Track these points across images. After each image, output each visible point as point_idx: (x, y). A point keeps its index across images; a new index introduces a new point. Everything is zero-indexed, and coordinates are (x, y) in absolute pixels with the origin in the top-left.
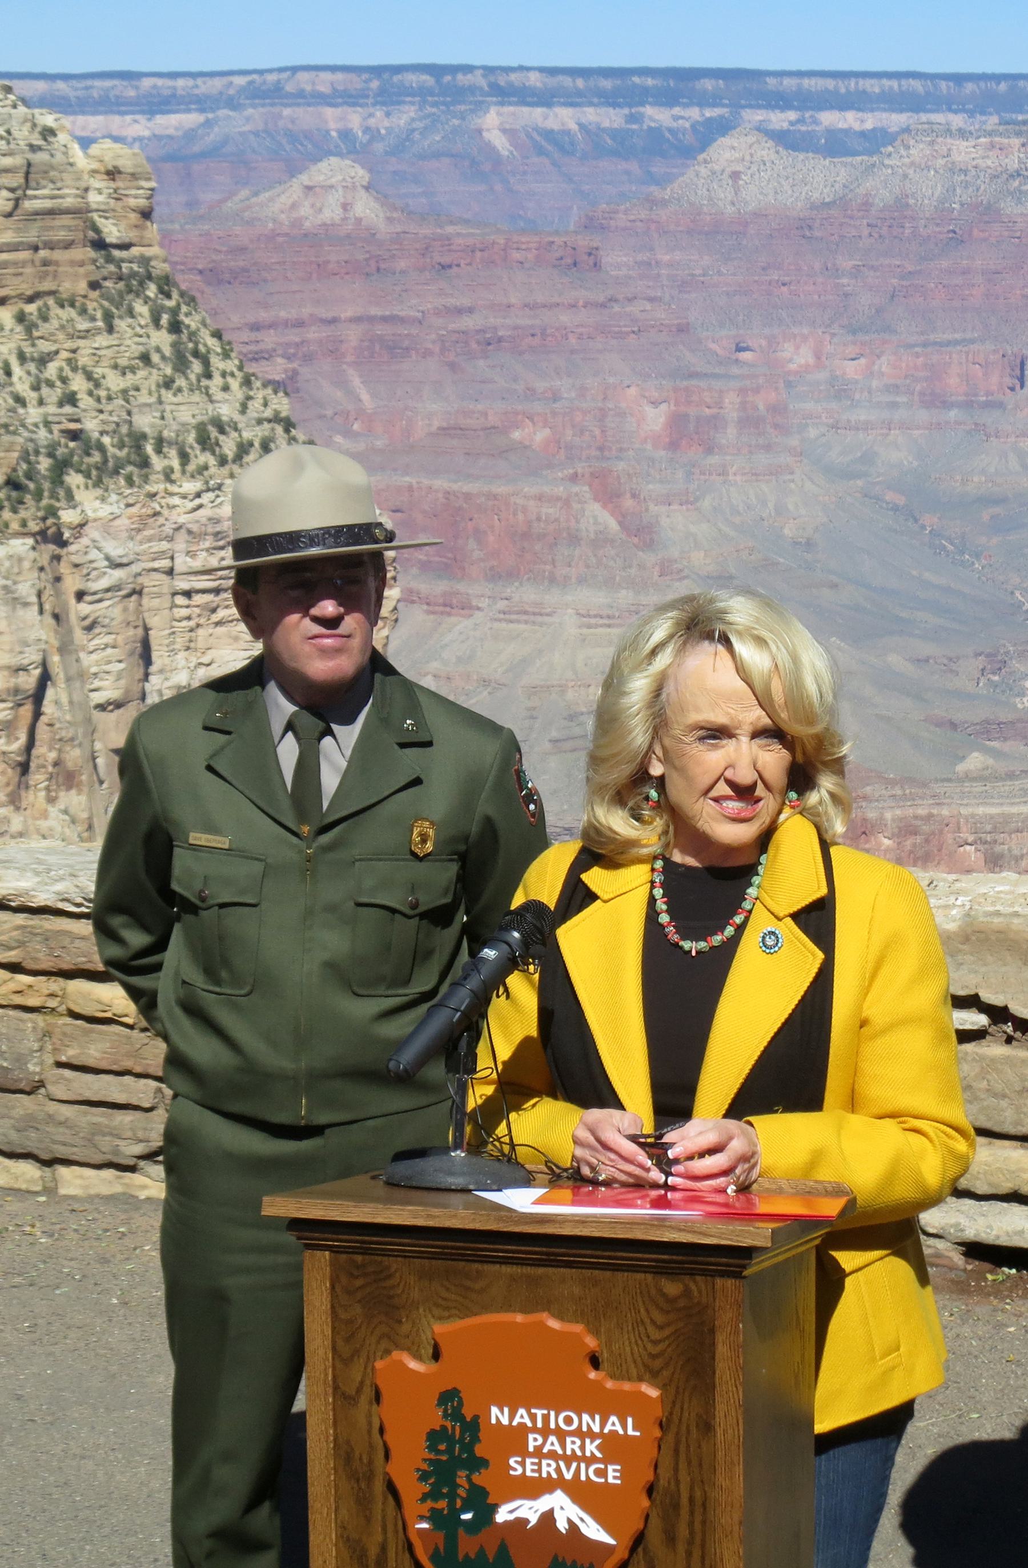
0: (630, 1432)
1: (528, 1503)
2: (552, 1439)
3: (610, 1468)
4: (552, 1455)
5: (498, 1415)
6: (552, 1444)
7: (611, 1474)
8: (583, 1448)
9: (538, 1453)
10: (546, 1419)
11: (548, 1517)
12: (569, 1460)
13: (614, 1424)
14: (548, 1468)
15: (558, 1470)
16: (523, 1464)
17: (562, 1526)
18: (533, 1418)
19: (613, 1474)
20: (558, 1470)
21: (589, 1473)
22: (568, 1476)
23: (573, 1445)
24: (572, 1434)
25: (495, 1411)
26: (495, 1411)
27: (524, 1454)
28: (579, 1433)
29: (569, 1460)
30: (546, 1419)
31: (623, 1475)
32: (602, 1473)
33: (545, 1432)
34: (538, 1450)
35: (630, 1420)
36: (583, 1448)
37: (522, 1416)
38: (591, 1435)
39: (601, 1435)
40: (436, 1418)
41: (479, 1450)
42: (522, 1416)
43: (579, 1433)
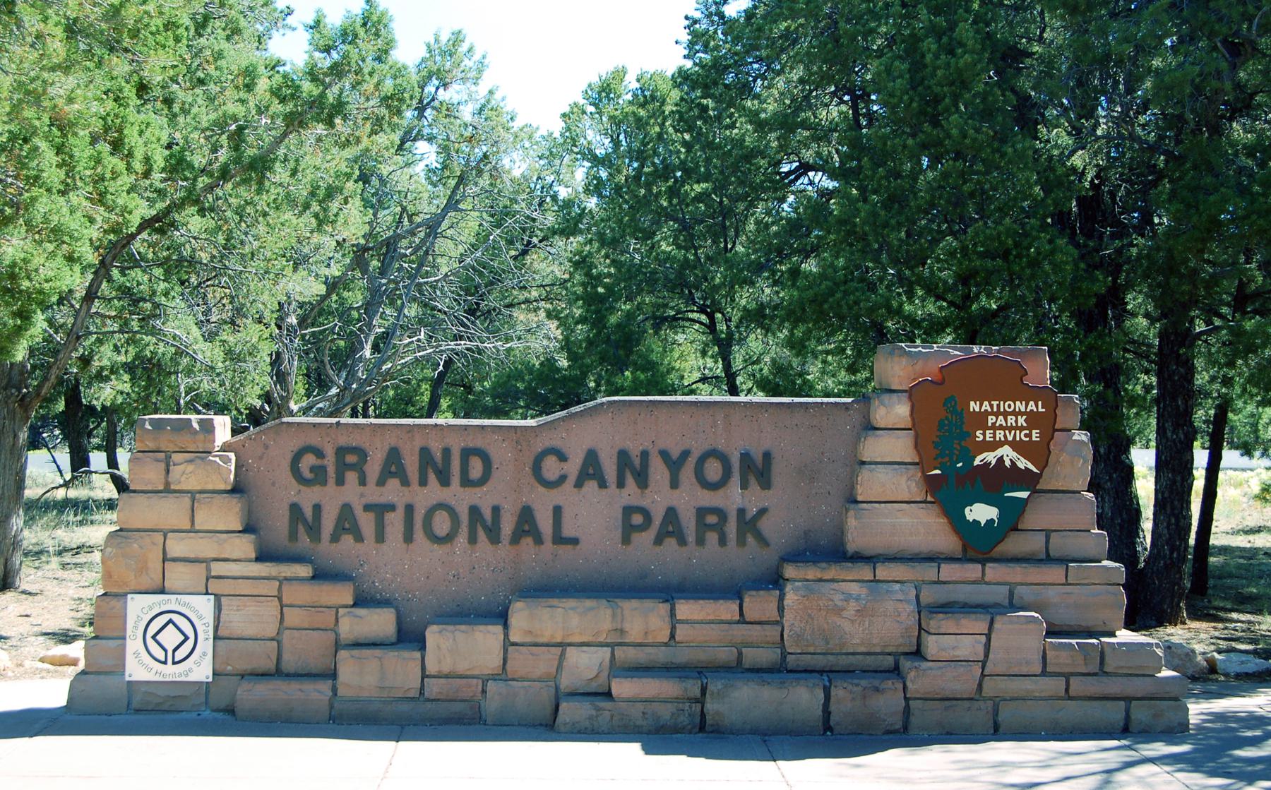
2: (1001, 417)
4: (1001, 427)
6: (1001, 421)
7: (1034, 435)
8: (1016, 421)
10: (998, 406)
11: (1001, 460)
12: (1010, 428)
14: (1000, 435)
15: (1005, 436)
16: (984, 434)
17: (1008, 463)
18: (992, 406)
20: (1005, 436)
21: (1021, 436)
22: (1010, 438)
23: (1011, 420)
25: (972, 403)
26: (972, 403)
27: (985, 428)
29: (1010, 428)
30: (998, 406)
32: (1029, 435)
33: (997, 414)
34: (994, 424)
36: (1016, 421)
37: (986, 404)
43: (1016, 414)
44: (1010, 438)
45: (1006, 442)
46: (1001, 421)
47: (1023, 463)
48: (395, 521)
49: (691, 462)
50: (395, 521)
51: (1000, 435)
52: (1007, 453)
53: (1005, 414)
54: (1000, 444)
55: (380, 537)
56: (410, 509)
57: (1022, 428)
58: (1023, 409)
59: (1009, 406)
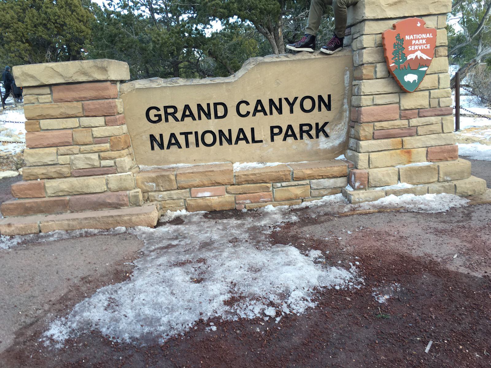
0: (431, 37)
1: (413, 54)
2: (417, 41)
3: (428, 45)
4: (417, 45)
5: (407, 38)
6: (417, 42)
9: (414, 45)
10: (416, 36)
11: (417, 56)
13: (428, 36)
14: (416, 47)
15: (418, 48)
17: (419, 57)
18: (414, 37)
19: (428, 46)
20: (418, 48)
21: (424, 47)
22: (420, 48)
23: (421, 41)
24: (421, 39)
25: (407, 37)
26: (407, 37)
27: (412, 45)
28: (422, 39)
30: (416, 36)
31: (431, 46)
32: (426, 47)
33: (416, 40)
34: (414, 44)
35: (431, 34)
37: (412, 37)
38: (424, 39)
39: (426, 38)
40: (395, 41)
41: (404, 46)
42: (412, 37)
43: (422, 39)
44: (420, 48)
45: (419, 50)
46: (417, 42)
47: (425, 57)
48: (192, 138)
49: (298, 101)
50: (192, 138)
51: (416, 47)
52: (419, 54)
53: (419, 39)
54: (416, 51)
55: (187, 145)
56: (196, 133)
57: (424, 44)
58: (425, 37)
59: (420, 36)
